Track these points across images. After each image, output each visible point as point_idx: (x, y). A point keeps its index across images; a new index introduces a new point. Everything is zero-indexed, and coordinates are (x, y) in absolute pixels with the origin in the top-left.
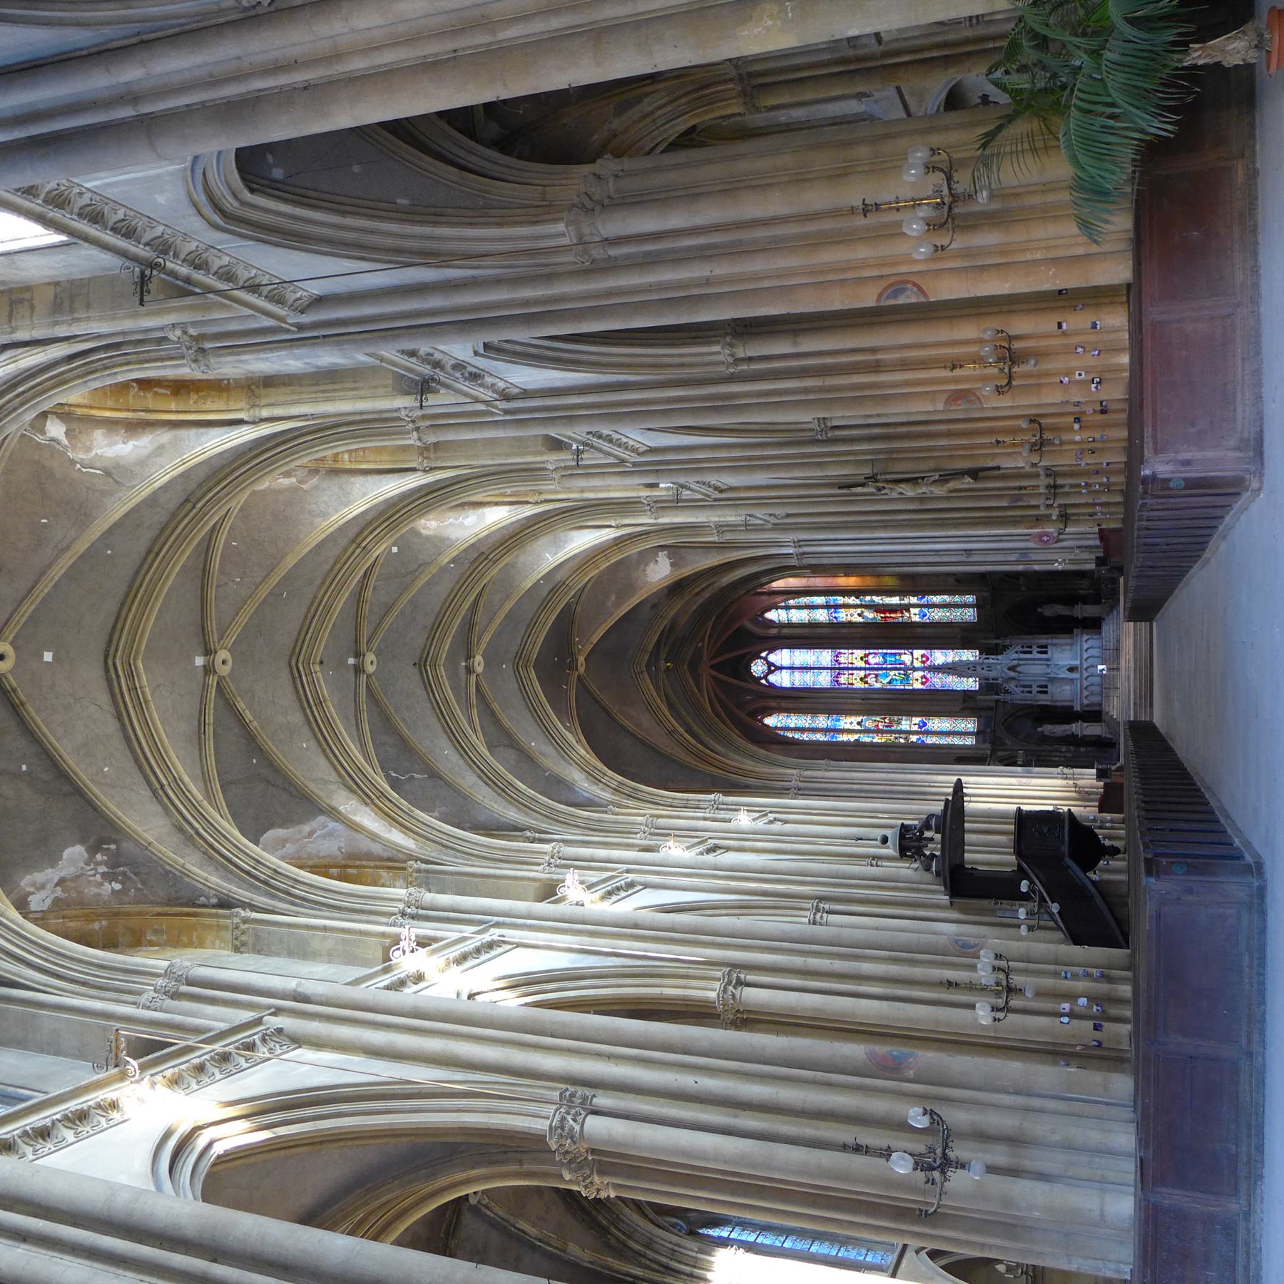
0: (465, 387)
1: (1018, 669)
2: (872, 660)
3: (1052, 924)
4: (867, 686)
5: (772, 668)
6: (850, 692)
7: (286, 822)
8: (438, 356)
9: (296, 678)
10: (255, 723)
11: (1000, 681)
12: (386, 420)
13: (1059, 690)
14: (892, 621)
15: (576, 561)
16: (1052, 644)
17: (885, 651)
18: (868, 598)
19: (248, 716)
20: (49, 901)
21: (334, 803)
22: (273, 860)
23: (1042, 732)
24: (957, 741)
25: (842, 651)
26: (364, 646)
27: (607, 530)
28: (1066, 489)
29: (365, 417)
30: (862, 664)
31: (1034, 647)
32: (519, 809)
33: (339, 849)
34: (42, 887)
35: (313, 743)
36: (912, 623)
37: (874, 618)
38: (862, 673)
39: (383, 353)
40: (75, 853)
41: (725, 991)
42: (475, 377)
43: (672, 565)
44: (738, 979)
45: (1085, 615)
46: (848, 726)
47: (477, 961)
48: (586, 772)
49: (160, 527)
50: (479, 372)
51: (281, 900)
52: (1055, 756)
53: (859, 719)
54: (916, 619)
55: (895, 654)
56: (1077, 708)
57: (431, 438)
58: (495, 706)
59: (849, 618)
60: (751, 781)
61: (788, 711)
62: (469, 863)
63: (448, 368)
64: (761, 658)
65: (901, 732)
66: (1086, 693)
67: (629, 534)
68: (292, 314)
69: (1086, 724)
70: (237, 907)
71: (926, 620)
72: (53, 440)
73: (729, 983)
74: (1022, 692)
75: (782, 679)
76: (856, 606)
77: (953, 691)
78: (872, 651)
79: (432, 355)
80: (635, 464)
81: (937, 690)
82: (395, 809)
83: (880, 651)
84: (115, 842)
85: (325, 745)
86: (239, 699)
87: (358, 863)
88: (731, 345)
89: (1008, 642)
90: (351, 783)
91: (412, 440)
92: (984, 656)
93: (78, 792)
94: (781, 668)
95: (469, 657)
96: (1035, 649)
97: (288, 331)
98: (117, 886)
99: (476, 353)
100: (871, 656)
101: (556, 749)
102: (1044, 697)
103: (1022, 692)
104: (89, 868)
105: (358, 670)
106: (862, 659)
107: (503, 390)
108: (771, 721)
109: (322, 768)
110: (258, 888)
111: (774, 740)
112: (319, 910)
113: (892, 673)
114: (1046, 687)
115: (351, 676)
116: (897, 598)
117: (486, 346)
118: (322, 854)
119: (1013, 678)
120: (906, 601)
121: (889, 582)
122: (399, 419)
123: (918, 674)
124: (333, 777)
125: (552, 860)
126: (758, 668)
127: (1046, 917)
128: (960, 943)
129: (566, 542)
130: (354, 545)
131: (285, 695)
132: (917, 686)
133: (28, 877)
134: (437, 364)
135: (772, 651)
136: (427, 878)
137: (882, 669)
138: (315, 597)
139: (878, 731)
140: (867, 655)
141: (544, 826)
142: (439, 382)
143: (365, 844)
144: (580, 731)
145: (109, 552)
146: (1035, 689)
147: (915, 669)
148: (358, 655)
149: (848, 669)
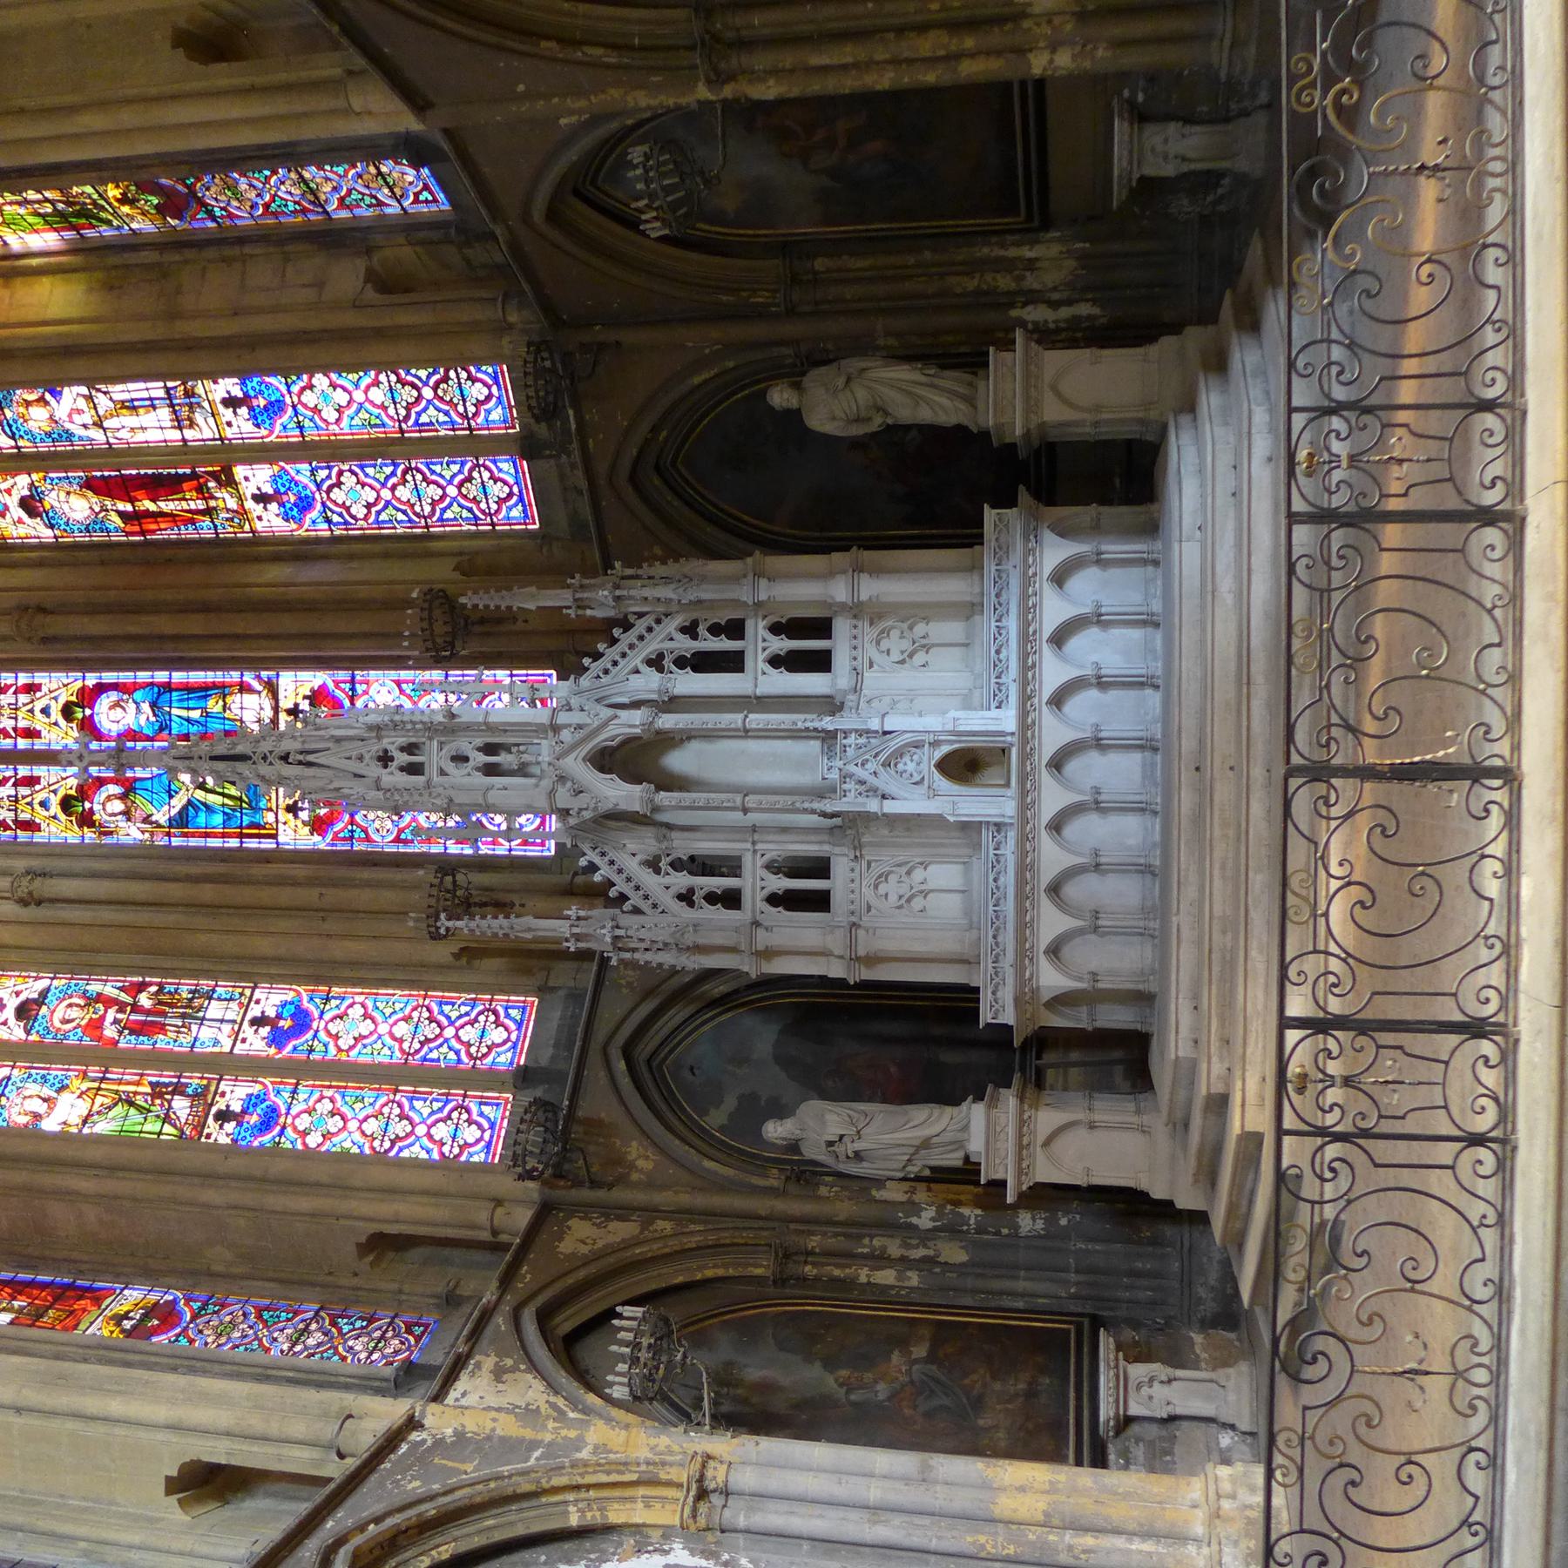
1: (678, 761)
2: (111, 716)
4: (89, 835)
13: (891, 887)
14: (168, 533)
16: (856, 610)
17: (161, 676)
23: (794, 1147)
31: (757, 629)
36: (257, 540)
45: (1053, 412)
52: (879, 1260)
54: (270, 521)
55: (204, 690)
65: (193, 1061)
66: (1051, 922)
71: (314, 525)
74: (687, 897)
78: (109, 677)
83: (143, 676)
89: (602, 601)
96: (760, 643)
100: (105, 701)
102: (801, 929)
103: (687, 897)
114: (821, 868)
140: (89, 697)
146: (756, 882)
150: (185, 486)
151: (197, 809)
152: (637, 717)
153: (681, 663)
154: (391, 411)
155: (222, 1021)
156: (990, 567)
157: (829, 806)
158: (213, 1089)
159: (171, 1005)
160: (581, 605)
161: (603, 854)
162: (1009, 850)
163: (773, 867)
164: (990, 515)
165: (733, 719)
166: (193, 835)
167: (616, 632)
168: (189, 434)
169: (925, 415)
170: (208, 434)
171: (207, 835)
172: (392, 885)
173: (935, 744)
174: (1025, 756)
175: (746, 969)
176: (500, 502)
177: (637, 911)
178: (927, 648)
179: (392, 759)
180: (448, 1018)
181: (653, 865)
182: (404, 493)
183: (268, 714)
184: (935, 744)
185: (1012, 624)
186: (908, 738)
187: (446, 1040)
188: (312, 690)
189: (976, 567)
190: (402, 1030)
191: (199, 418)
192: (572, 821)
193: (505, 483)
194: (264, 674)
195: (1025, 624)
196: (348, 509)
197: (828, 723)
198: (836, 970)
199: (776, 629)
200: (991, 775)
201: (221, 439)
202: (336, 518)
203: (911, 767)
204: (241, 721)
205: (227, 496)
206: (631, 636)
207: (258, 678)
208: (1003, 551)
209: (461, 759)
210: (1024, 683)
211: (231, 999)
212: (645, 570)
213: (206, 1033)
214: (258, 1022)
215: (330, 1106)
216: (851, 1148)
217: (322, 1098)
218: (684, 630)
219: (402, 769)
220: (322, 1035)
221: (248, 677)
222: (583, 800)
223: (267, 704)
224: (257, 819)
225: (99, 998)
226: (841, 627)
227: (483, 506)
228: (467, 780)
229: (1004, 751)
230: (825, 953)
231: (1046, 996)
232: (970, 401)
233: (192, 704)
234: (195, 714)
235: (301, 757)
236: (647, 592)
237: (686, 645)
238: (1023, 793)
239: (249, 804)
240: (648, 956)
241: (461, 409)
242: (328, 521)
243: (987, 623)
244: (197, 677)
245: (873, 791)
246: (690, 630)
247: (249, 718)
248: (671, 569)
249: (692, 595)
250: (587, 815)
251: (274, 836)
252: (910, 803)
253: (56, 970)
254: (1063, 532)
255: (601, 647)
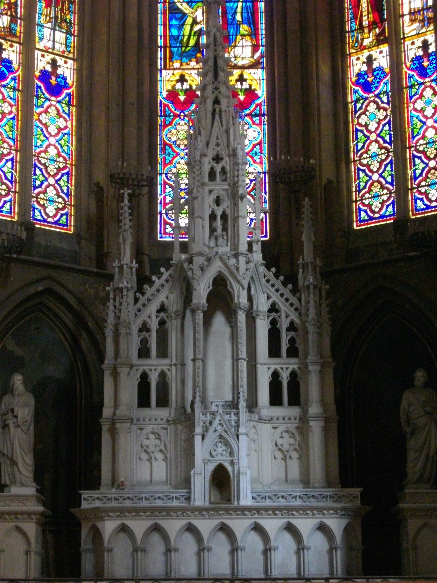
13: (152, 442)
36: (345, 56)
74: (145, 328)
103: (145, 328)
150: (377, 14)
151: (181, 19)
152: (243, 300)
153: (273, 323)
154: (421, 142)
155: (54, 41)
156: (328, 492)
157: (198, 405)
158: (15, 39)
159: (62, 10)
160: (305, 266)
161: (167, 281)
162: (175, 503)
163: (163, 375)
164: (357, 491)
165: (243, 353)
166: (165, 17)
167: (290, 286)
168: (407, 19)
169: (411, 455)
170: (407, 30)
171: (165, 25)
172: (139, 144)
173: (232, 463)
174: (227, 511)
175: (106, 362)
176: (370, 206)
177: (136, 300)
178: (284, 459)
179: (218, 163)
180: (60, 179)
181: (162, 309)
182: (374, 148)
183: (241, 63)
184: (232, 463)
185: (298, 503)
186: (235, 448)
187: (47, 180)
188: (255, 90)
189: (329, 484)
190: (52, 152)
191: (416, 25)
192: (186, 265)
193: (381, 209)
194: (264, 60)
195: (297, 509)
196: (364, 113)
197: (242, 404)
198: (107, 412)
199: (293, 375)
200: (215, 495)
201: (404, 38)
202: (359, 105)
203: (220, 450)
204: (235, 46)
205: (371, 39)
206: (288, 294)
207: (262, 56)
208: (337, 498)
209: (218, 202)
210: (266, 509)
211: (67, 46)
212: (325, 302)
213: (47, 32)
214: (54, 63)
215: (6, 111)
216: (10, 422)
217: (11, 106)
218: (292, 323)
219: (212, 168)
220: (47, 103)
221: (262, 50)
222: (198, 272)
223: (246, 62)
224: (176, 57)
226: (295, 411)
227: (367, 195)
228: (207, 206)
229: (229, 500)
230: (116, 405)
231: (99, 525)
232: (419, 480)
233: (245, 15)
234: (238, 17)
235: (217, 111)
236: (312, 303)
237: (284, 324)
238: (208, 510)
239: (185, 52)
240: (111, 308)
241: (423, 183)
242: (357, 101)
243: (298, 490)
244: (262, 18)
245: (206, 430)
246: (292, 327)
247: (238, 51)
248: (325, 316)
249: (311, 328)
250: (190, 273)
251: (165, 68)
254: (347, 530)
255: (282, 278)
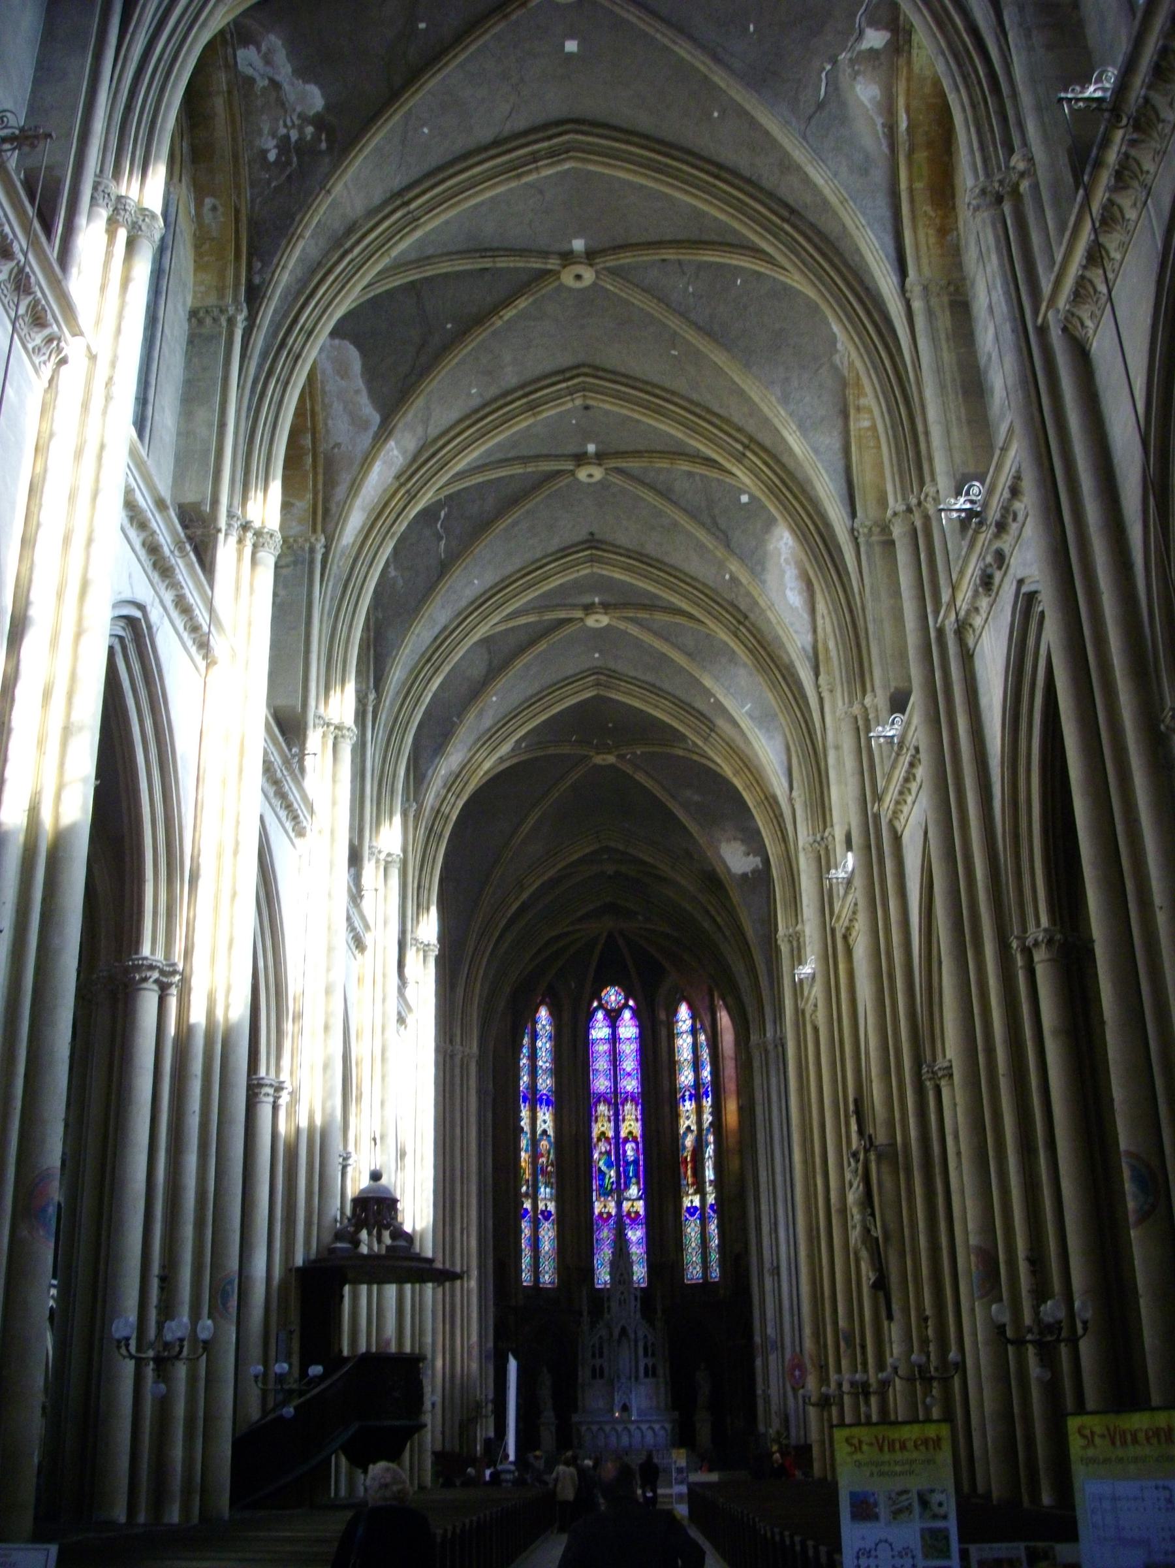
0: (973, 571)
2: (629, 1147)
3: (271, 1404)
4: (595, 1140)
5: (613, 1018)
6: (588, 1118)
7: (371, 374)
8: (1014, 527)
9: (563, 374)
10: (499, 323)
11: (607, 1316)
12: (920, 468)
14: (682, 1170)
15: (742, 745)
17: (641, 1163)
18: (711, 1138)
19: (509, 314)
20: (250, 71)
21: (397, 434)
22: (312, 354)
24: (526, 1261)
25: (640, 1107)
26: (613, 463)
27: (786, 785)
28: (863, 1409)
29: (922, 438)
30: (623, 1134)
32: (404, 684)
33: (338, 445)
34: (268, 61)
35: (476, 402)
37: (684, 1147)
38: (610, 1134)
39: (1012, 453)
40: (315, 99)
41: (151, 968)
42: (986, 582)
43: (744, 876)
44: (170, 985)
46: (540, 1115)
47: (181, 628)
48: (460, 772)
49: (754, 178)
50: (995, 588)
51: (260, 366)
53: (551, 1132)
54: (686, 1203)
56: (575, 1418)
57: (898, 531)
58: (542, 646)
59: (683, 1115)
60: (460, 991)
61: (557, 1038)
62: (325, 617)
63: (997, 544)
64: (627, 1001)
66: (595, 1428)
67: (782, 815)
68: (1061, 316)
69: (553, 1429)
70: (249, 310)
72: (861, 34)
73: (162, 972)
75: (599, 1032)
76: (699, 1122)
77: (593, 1255)
78: (641, 1146)
79: (1015, 519)
80: (877, 817)
81: (592, 1233)
82: (393, 515)
83: (641, 1157)
84: (330, 148)
85: (475, 418)
86: (531, 300)
87: (320, 470)
88: (1050, 942)
90: (426, 455)
91: (894, 504)
92: (638, 1294)
93: (393, 96)
94: (614, 1026)
95: (606, 607)
97: (1036, 312)
98: (272, 156)
99: (1021, 582)
100: (633, 1145)
101: (489, 730)
104: (295, 118)
105: (581, 459)
106: (630, 1133)
107: (971, 625)
108: (543, 1013)
109: (444, 416)
110: (275, 335)
111: (522, 1021)
112: (247, 417)
113: (613, 1173)
114: (602, 1376)
115: (571, 449)
116: (712, 1177)
117: (1031, 597)
118: (330, 422)
119: (611, 1335)
120: (709, 1189)
121: (734, 1164)
122: (922, 484)
123: (612, 1208)
124: (433, 432)
125: (332, 728)
126: (613, 996)
127: (280, 1397)
128: (228, 1288)
129: (768, 730)
130: (746, 441)
131: (541, 361)
132: (598, 1208)
133: (279, 43)
134: (1001, 527)
135: (636, 1015)
136: (303, 563)
137: (618, 1159)
138: (673, 393)
139: (535, 1155)
140: (635, 1140)
141: (383, 717)
142: (977, 532)
143: (345, 479)
144: (515, 761)
145: (716, 114)
146: (598, 1362)
147: (619, 1205)
148: (600, 457)
149: (617, 1114)
164: (677, 1413)
181: (601, 1337)
209: (622, 1293)
225: (549, 1153)
237: (649, 1344)
246: (653, 1344)
247: (631, 1191)
252: (617, 1398)
253: (556, 1137)
